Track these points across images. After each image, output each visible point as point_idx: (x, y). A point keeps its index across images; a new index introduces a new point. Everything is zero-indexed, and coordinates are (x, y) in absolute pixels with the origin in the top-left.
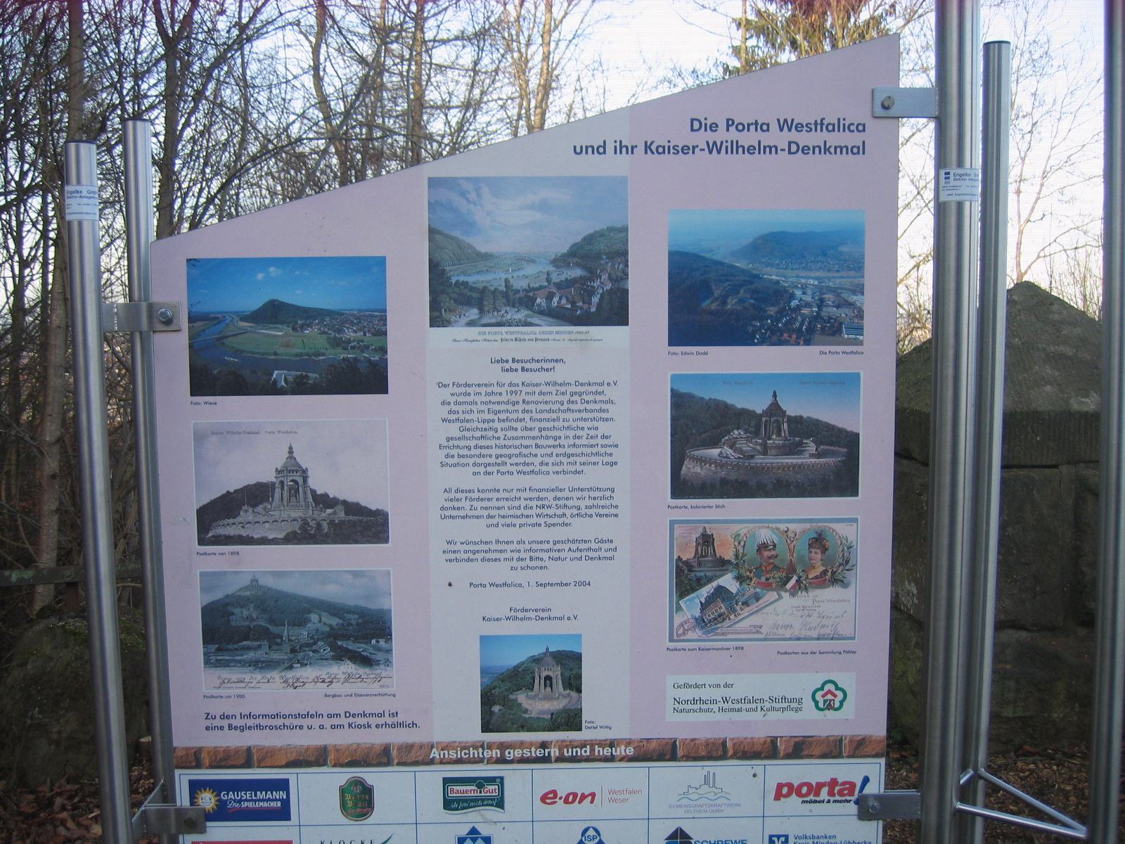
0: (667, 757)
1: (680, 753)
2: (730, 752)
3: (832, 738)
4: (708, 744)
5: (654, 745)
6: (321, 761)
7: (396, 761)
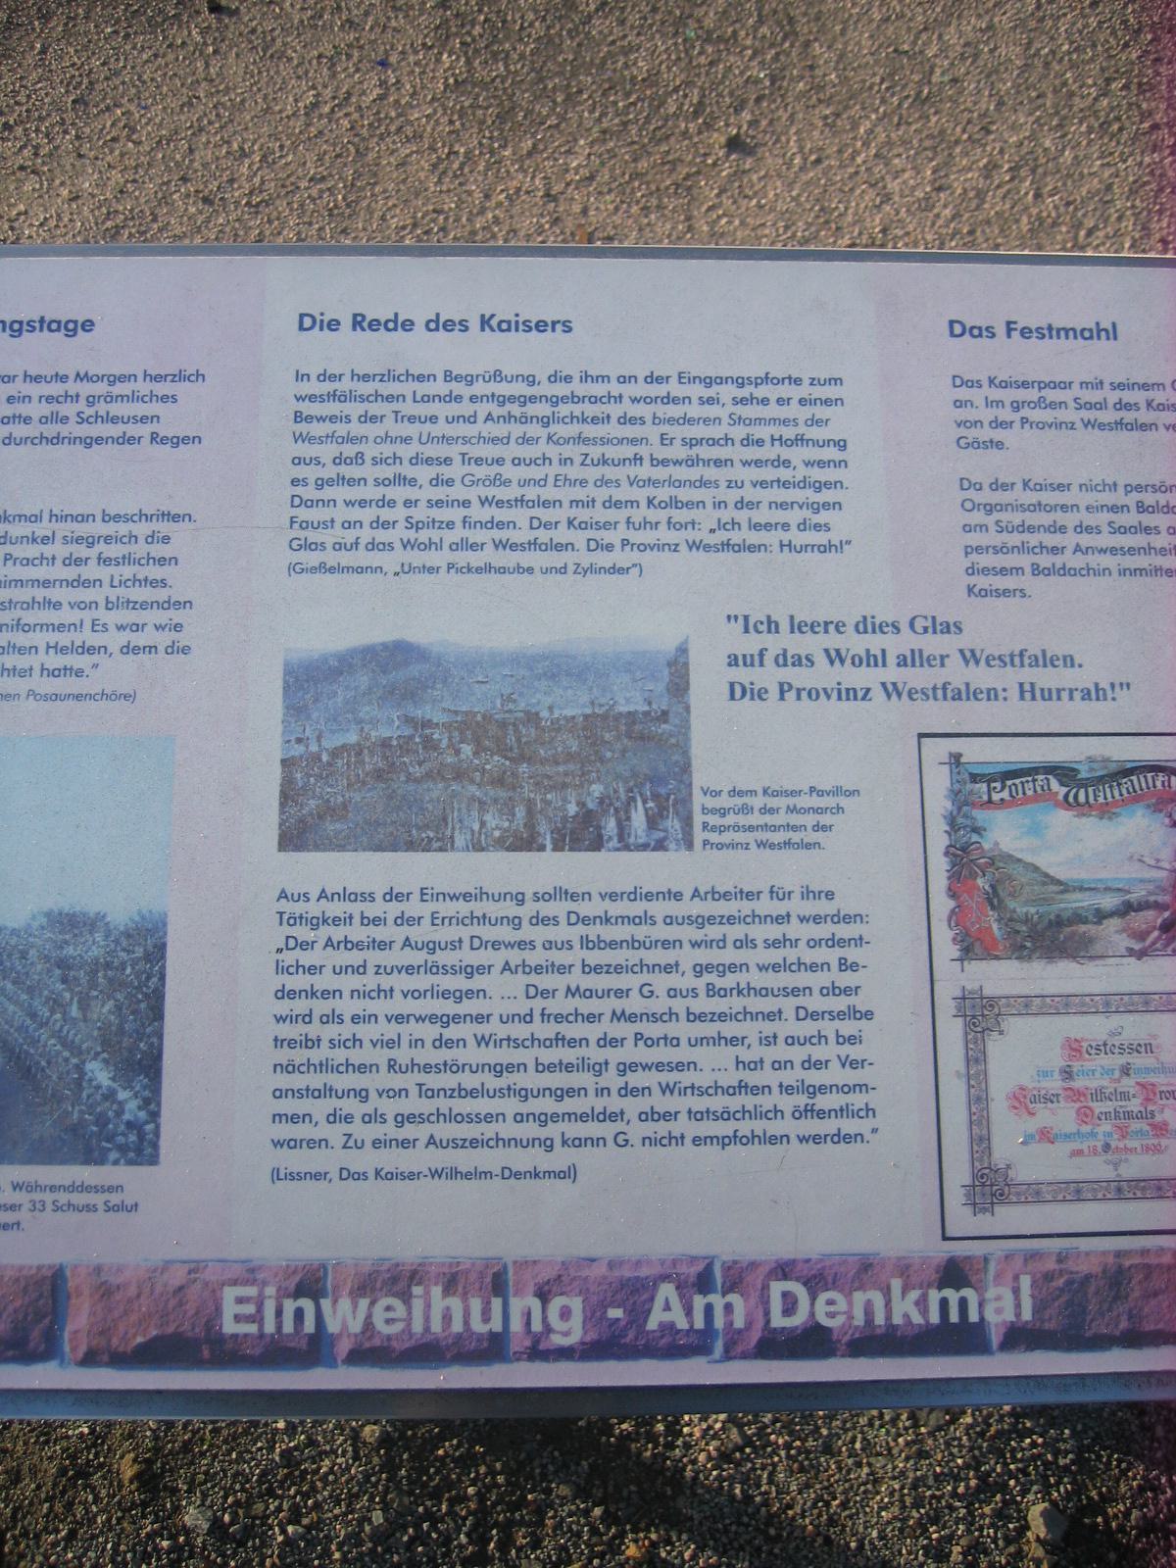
6: (36, 1334)
7: (344, 1347)
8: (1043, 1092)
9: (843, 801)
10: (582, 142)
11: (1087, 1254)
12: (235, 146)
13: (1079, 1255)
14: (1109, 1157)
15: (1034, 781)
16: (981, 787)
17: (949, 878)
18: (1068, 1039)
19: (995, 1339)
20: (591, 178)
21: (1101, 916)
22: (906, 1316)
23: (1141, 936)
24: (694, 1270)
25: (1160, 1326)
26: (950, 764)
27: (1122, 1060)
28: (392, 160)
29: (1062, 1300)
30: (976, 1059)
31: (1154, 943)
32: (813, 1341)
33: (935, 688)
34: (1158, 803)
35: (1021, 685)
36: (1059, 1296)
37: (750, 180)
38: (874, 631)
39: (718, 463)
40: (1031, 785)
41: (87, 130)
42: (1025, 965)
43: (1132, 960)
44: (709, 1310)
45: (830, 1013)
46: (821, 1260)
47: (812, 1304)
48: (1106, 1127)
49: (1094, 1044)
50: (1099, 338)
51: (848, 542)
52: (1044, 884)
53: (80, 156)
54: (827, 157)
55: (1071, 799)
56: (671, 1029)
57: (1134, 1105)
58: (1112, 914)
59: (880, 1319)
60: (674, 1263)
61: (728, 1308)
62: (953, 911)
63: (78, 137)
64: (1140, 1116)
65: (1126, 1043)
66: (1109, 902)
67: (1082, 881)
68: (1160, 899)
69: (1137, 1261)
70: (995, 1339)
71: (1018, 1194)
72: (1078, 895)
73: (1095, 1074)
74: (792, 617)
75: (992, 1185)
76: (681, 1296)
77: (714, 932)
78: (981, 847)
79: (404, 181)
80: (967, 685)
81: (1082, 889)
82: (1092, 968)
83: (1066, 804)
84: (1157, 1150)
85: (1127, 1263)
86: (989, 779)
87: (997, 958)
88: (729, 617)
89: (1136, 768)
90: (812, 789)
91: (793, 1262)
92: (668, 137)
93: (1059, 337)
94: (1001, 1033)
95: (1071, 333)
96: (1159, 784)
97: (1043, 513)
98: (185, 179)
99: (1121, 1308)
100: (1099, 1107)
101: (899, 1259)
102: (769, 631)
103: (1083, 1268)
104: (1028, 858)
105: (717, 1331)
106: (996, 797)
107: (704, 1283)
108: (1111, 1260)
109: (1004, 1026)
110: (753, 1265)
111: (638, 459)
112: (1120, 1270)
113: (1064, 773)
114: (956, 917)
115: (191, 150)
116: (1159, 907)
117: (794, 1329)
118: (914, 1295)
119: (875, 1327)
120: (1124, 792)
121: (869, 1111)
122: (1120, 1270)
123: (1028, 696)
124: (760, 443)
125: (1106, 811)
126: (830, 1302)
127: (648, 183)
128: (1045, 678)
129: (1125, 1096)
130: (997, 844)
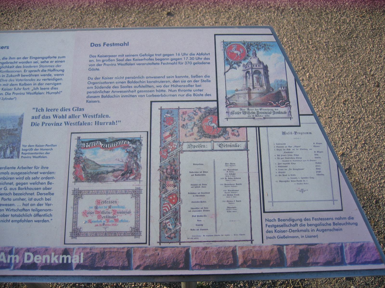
0: (181, 266)
1: (193, 261)
2: (240, 261)
3: (333, 246)
4: (219, 253)
5: (167, 254)
9: (53, 147)
10: (133, 14)
11: (97, 248)
12: (54, 17)
13: (95, 248)
14: (104, 226)
15: (96, 143)
16: (83, 144)
18: (97, 200)
19: (74, 267)
20: (135, 22)
21: (108, 172)
22: (54, 261)
23: (116, 177)
24: (8, 250)
25: (112, 265)
28: (89, 20)
29: (90, 258)
30: (76, 204)
31: (119, 179)
32: (33, 266)
33: (76, 123)
34: (124, 147)
35: (96, 122)
36: (89, 258)
37: (172, 22)
38: (64, 111)
39: (36, 76)
41: (21, 15)
43: (114, 182)
44: (11, 258)
45: (44, 194)
46: (37, 248)
47: (34, 258)
50: (124, 45)
51: (61, 92)
52: (95, 165)
53: (18, 20)
54: (191, 16)
55: (104, 147)
56: (10, 197)
57: (111, 215)
58: (110, 172)
59: (48, 262)
60: (5, 248)
61: (15, 258)
62: (74, 172)
63: (18, 16)
64: (112, 217)
66: (110, 169)
67: (104, 165)
68: (122, 169)
69: (108, 250)
70: (74, 267)
71: (82, 234)
72: (103, 168)
73: (102, 208)
74: (47, 108)
76: (5, 255)
77: (21, 176)
79: (91, 25)
80: (84, 122)
81: (104, 166)
82: (104, 184)
84: (115, 225)
85: (106, 251)
86: (86, 142)
87: (83, 182)
88: (33, 108)
90: (46, 145)
91: (30, 248)
92: (154, 13)
93: (115, 46)
94: (82, 198)
95: (118, 45)
96: (125, 143)
97: (106, 84)
98: (41, 25)
99: (104, 261)
100: (103, 215)
101: (54, 248)
102: (42, 111)
103: (95, 251)
104: (93, 160)
105: (12, 263)
107: (10, 253)
108: (102, 250)
110: (22, 249)
111: (19, 75)
112: (104, 252)
113: (103, 141)
114: (75, 173)
115: (43, 19)
116: (121, 170)
117: (29, 263)
118: (57, 256)
119: (47, 264)
120: (116, 145)
121: (51, 215)
122: (104, 252)
123: (97, 124)
124: (45, 71)
125: (112, 149)
126: (38, 257)
127: (147, 24)
128: (101, 120)
129: (109, 213)
130: (86, 156)
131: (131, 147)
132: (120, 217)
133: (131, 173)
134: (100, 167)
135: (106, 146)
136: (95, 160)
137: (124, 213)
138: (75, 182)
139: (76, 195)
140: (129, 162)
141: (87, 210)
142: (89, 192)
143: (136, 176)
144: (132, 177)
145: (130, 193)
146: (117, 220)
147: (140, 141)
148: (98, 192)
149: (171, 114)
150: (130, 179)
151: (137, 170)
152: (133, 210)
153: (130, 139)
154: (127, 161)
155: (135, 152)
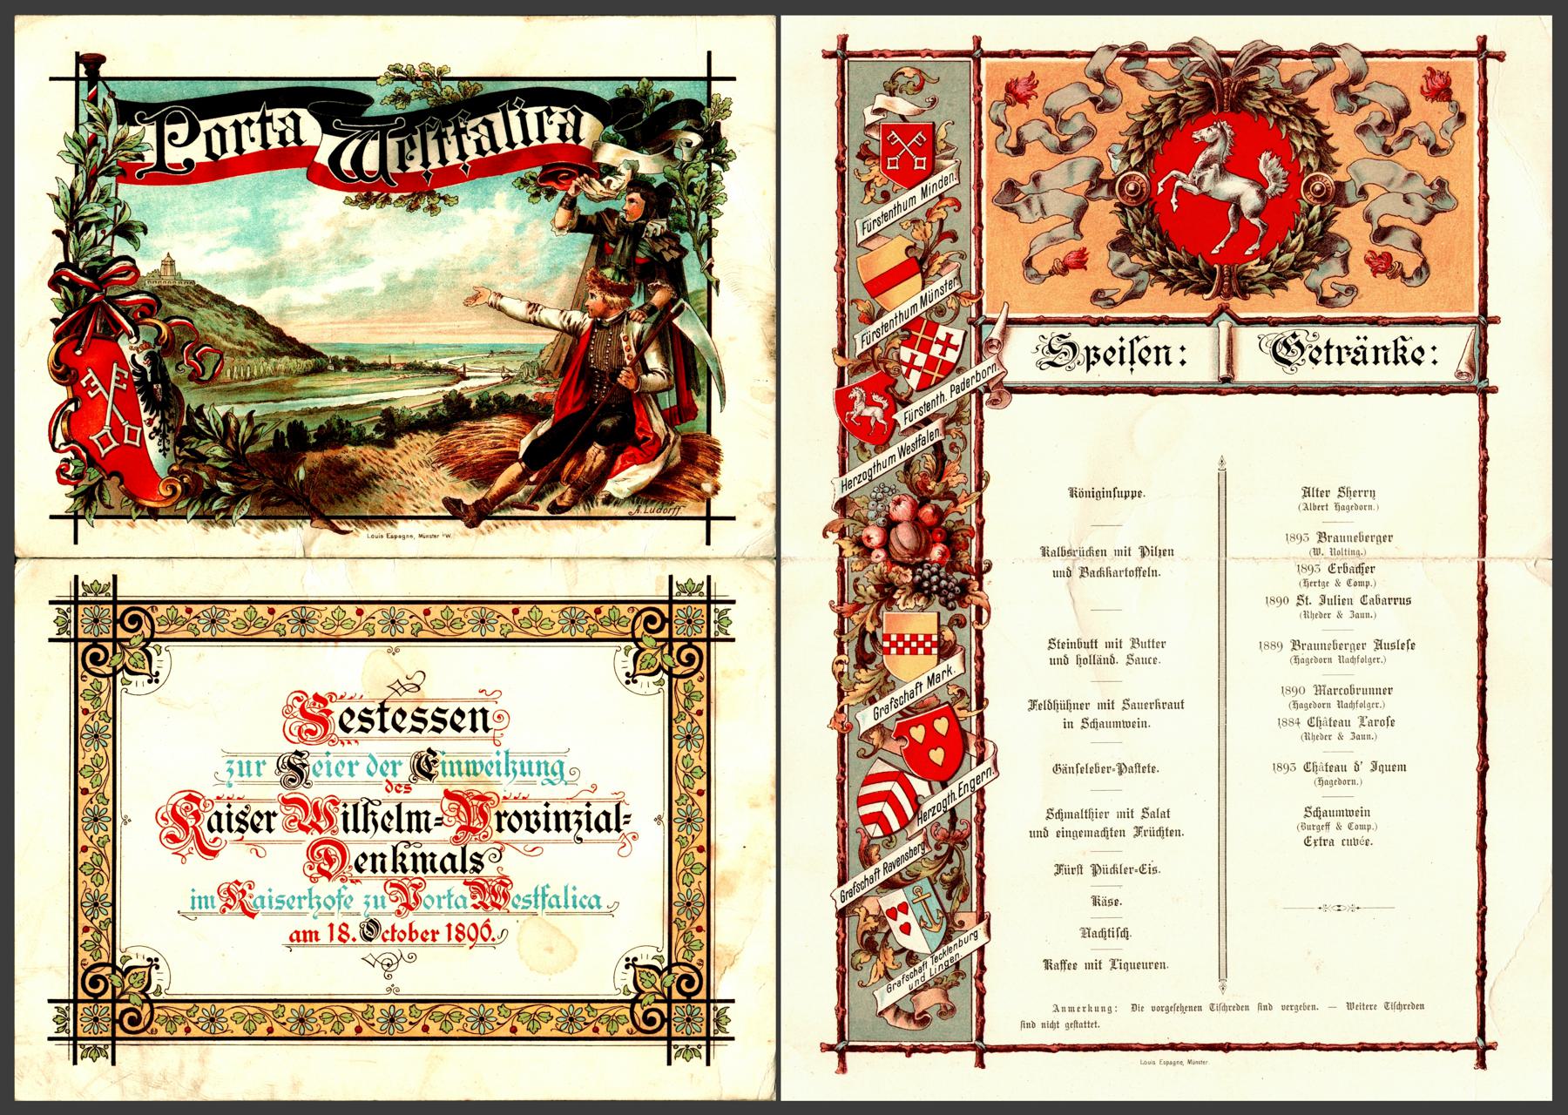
8: (236, 809)
14: (377, 949)
15: (264, 120)
16: (131, 132)
17: (57, 338)
18: (300, 695)
21: (393, 426)
23: (483, 473)
26: (77, 79)
27: (409, 746)
34: (544, 177)
40: (256, 128)
42: (216, 530)
43: (459, 525)
48: (372, 885)
49: (357, 708)
52: (271, 353)
55: (345, 163)
57: (438, 841)
58: (416, 426)
62: (62, 409)
64: (450, 866)
65: (431, 708)
66: (416, 396)
67: (353, 348)
68: (530, 391)
71: (171, 1020)
72: (346, 381)
73: (352, 771)
75: (114, 1001)
78: (135, 269)
81: (353, 365)
82: (363, 540)
83: (328, 176)
84: (480, 936)
87: (154, 514)
89: (510, 95)
94: (154, 678)
96: (552, 135)
100: (357, 845)
104: (238, 300)
106: (174, 156)
109: (160, 662)
113: (337, 104)
114: (73, 423)
116: (526, 410)
125: (422, 190)
129: (418, 821)
130: (169, 263)
131: (611, 170)
132: (525, 864)
133: (627, 441)
134: (318, 370)
135: (370, 162)
136: (264, 305)
137: (561, 821)
138: (76, 518)
139: (95, 642)
140: (595, 325)
141: (210, 793)
142: (210, 620)
143: (667, 475)
144: (640, 475)
145: (612, 631)
146: (493, 894)
147: (706, 116)
148: (298, 622)
149: (920, 97)
150: (609, 500)
151: (682, 412)
152: (647, 802)
153: (607, 92)
154: (576, 316)
155: (657, 226)
